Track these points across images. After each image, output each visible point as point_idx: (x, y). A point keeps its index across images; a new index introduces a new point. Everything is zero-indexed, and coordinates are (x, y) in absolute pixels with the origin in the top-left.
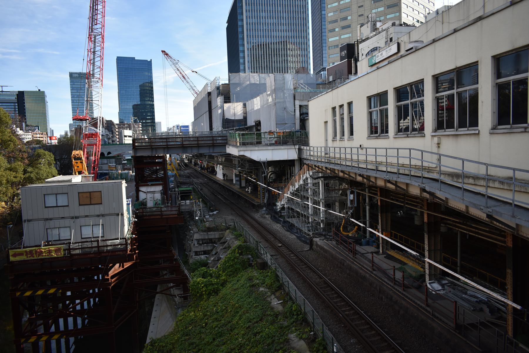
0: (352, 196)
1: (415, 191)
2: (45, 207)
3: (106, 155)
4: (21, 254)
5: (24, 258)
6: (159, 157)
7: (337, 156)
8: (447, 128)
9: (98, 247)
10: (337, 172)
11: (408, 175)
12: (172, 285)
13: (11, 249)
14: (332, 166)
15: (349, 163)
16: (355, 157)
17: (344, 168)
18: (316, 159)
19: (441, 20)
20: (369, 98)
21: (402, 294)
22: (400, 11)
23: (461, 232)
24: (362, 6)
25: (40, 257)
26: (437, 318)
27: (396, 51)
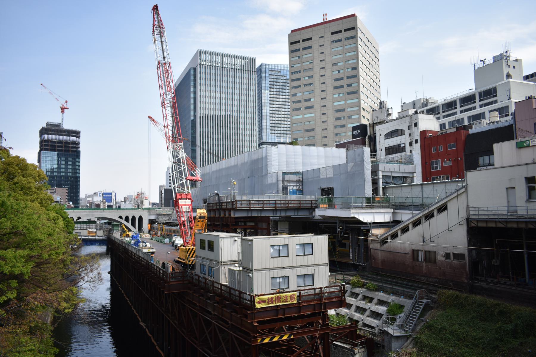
22: (359, 98)
24: (325, 91)
25: (278, 304)
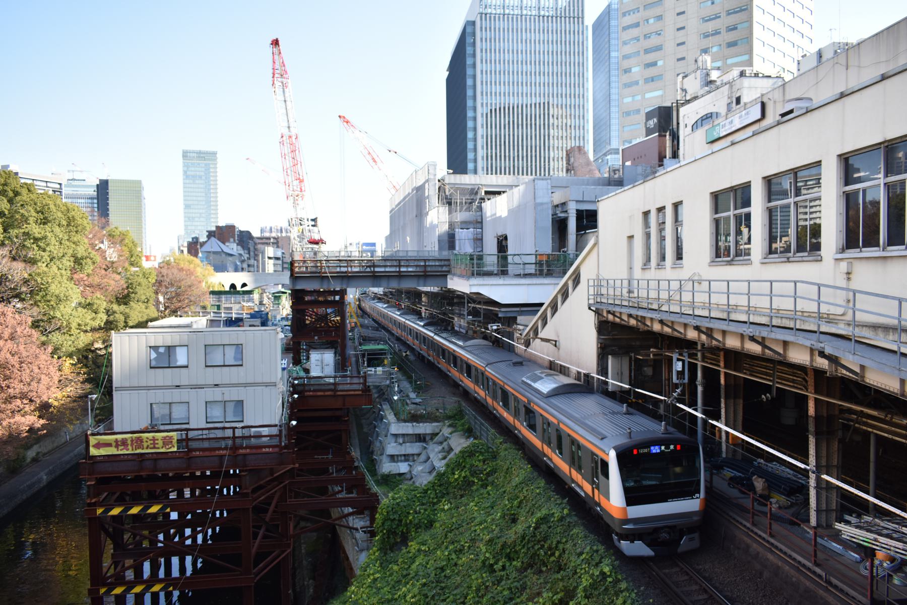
0: (680, 364)
1: (799, 357)
2: (151, 368)
3: (239, 288)
4: (108, 445)
5: (112, 451)
6: (335, 293)
7: (653, 294)
8: (864, 246)
9: (234, 438)
10: (649, 323)
11: (792, 329)
12: (351, 510)
13: (93, 434)
14: (641, 313)
15: (675, 308)
16: (687, 297)
17: (665, 317)
18: (611, 301)
19: (844, 63)
20: (716, 196)
21: (768, 542)
22: (750, 52)
23: (876, 434)
24: (683, 43)
26: (836, 587)
27: (759, 116)
